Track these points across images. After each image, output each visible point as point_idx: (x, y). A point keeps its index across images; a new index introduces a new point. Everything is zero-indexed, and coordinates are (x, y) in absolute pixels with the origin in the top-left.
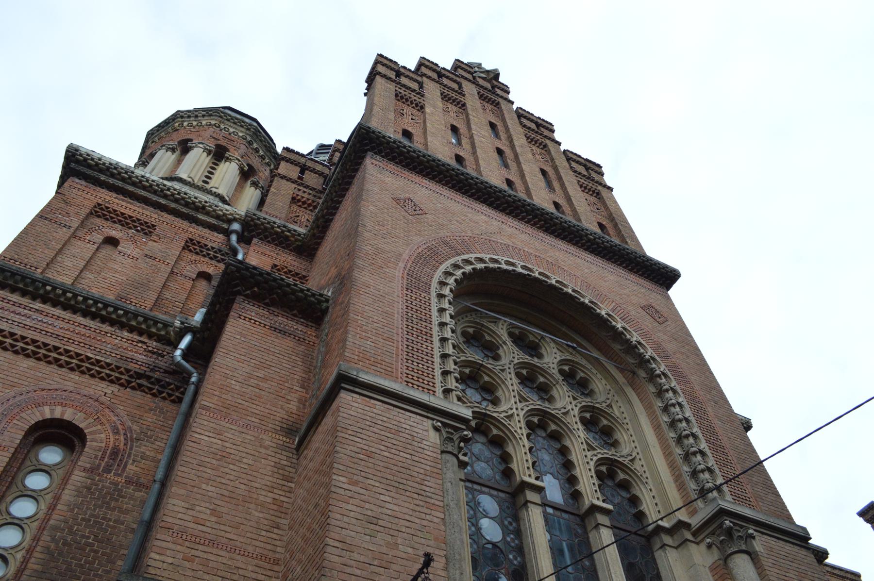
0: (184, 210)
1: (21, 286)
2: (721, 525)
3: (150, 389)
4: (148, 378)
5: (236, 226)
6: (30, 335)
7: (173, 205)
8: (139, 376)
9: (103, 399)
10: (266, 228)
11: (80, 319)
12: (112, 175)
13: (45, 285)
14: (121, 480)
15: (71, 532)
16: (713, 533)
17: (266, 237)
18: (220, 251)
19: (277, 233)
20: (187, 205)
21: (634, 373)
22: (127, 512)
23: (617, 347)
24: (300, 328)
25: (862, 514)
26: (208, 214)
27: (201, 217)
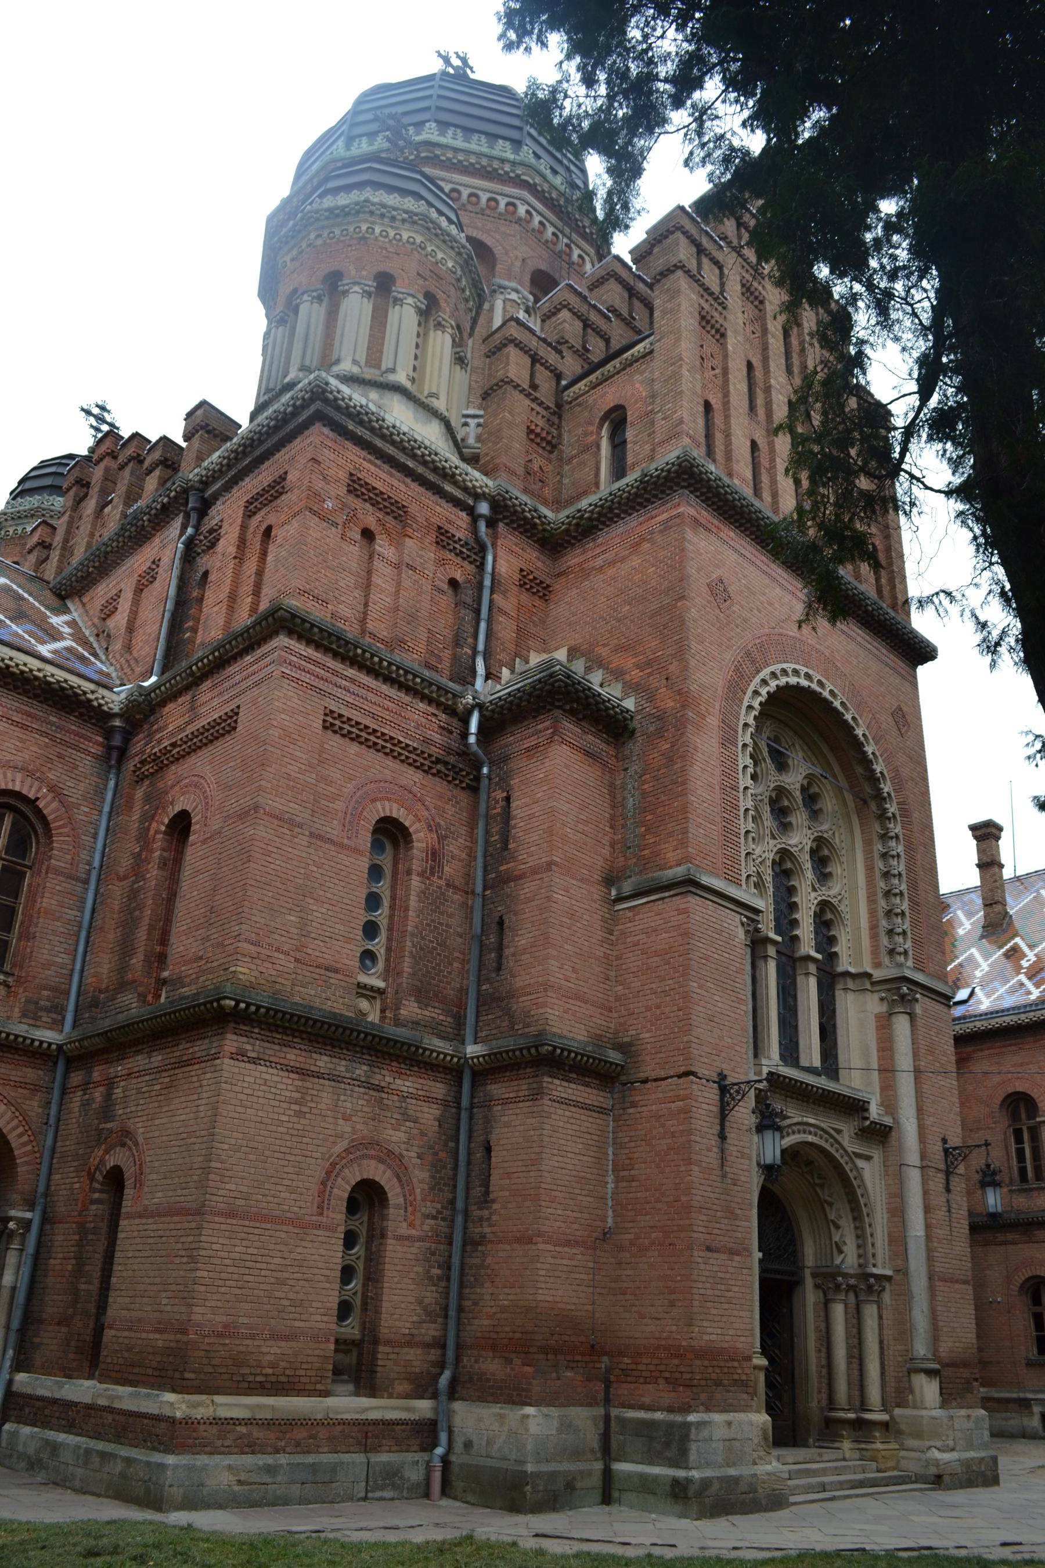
0: (431, 477)
1: (334, 646)
2: (899, 988)
3: (447, 775)
4: (446, 763)
5: (484, 508)
6: (356, 716)
7: (420, 470)
8: (438, 761)
9: (415, 789)
10: (516, 512)
11: (385, 688)
12: (361, 423)
13: (356, 647)
14: (442, 882)
15: (423, 938)
16: (889, 990)
17: (512, 522)
18: (467, 544)
19: (525, 518)
20: (435, 470)
21: (865, 802)
22: (450, 916)
23: (859, 770)
24: (603, 746)
25: (973, 828)
26: (455, 483)
27: (448, 488)
